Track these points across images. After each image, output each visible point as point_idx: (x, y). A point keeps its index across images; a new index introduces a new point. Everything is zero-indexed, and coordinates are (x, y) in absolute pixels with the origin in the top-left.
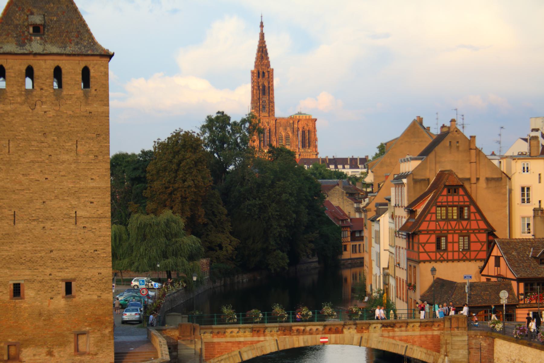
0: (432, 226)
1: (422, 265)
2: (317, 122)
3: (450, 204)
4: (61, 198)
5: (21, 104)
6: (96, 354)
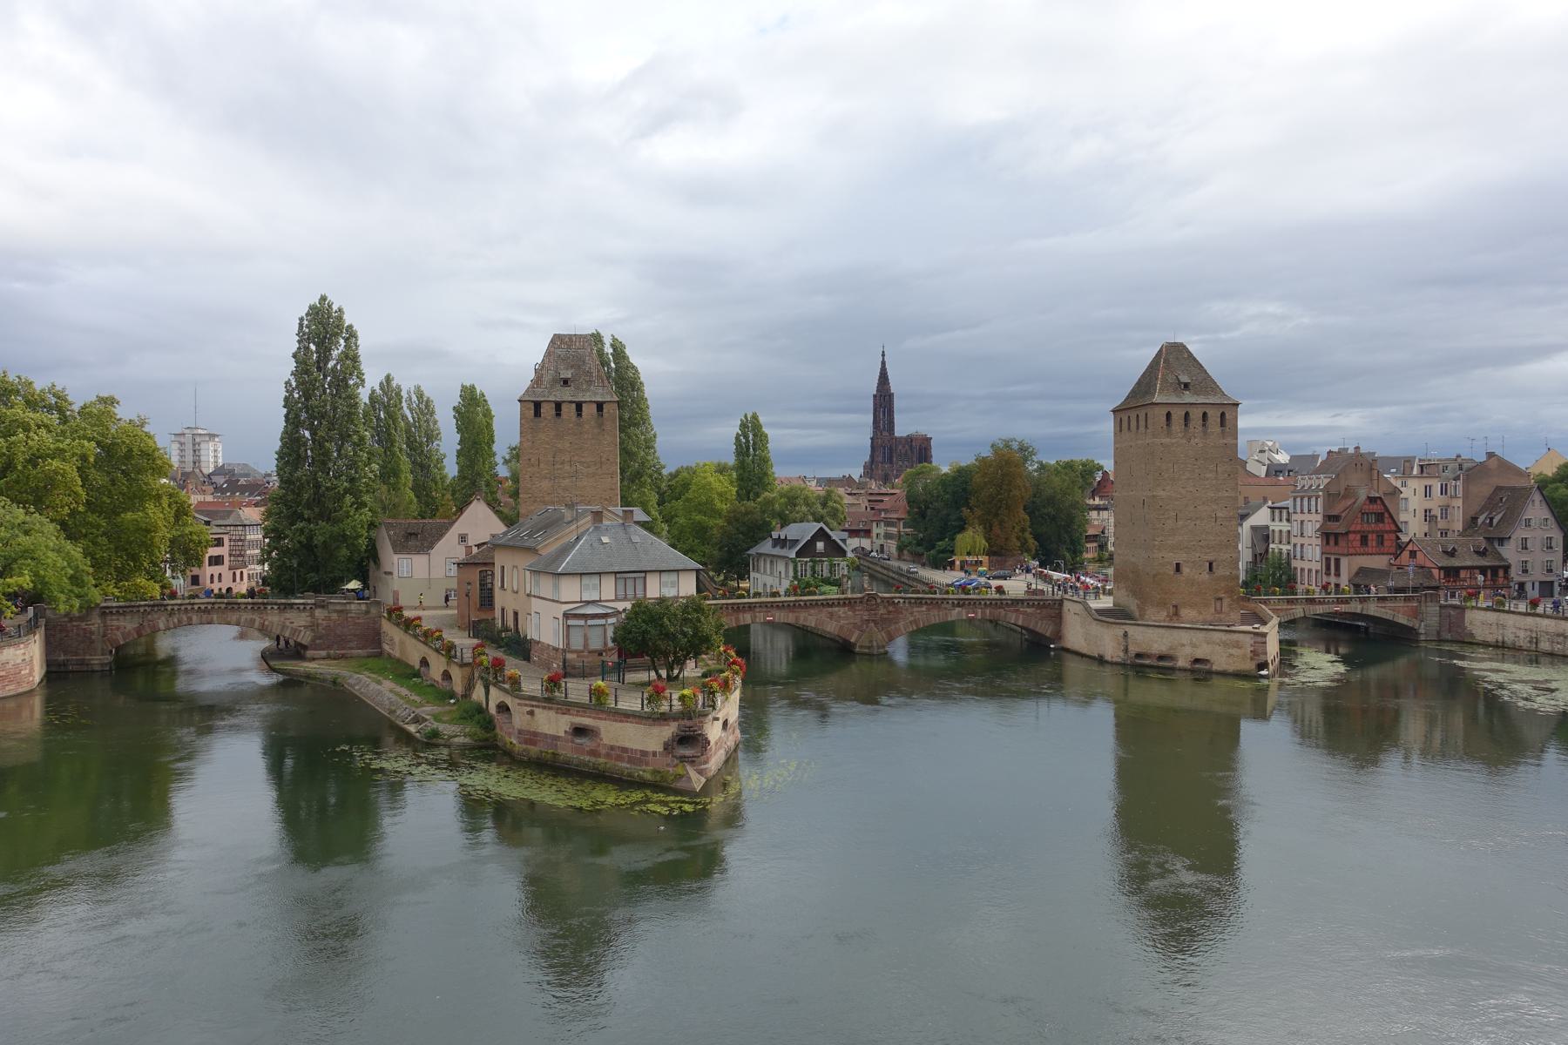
0: (1358, 528)
2: (932, 441)
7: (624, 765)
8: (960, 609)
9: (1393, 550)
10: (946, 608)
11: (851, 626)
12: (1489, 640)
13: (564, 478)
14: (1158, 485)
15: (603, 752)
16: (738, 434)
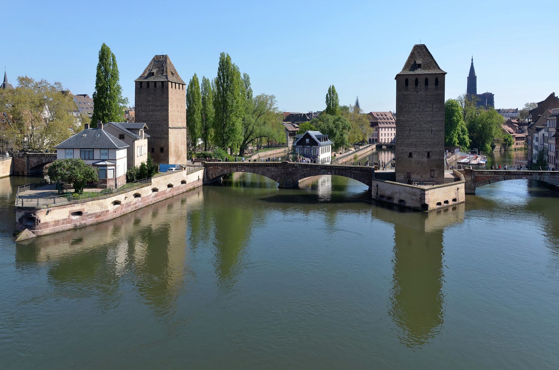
6: (438, 178)
8: (325, 170)
10: (318, 170)
11: (276, 175)
13: (150, 111)
16: (327, 94)
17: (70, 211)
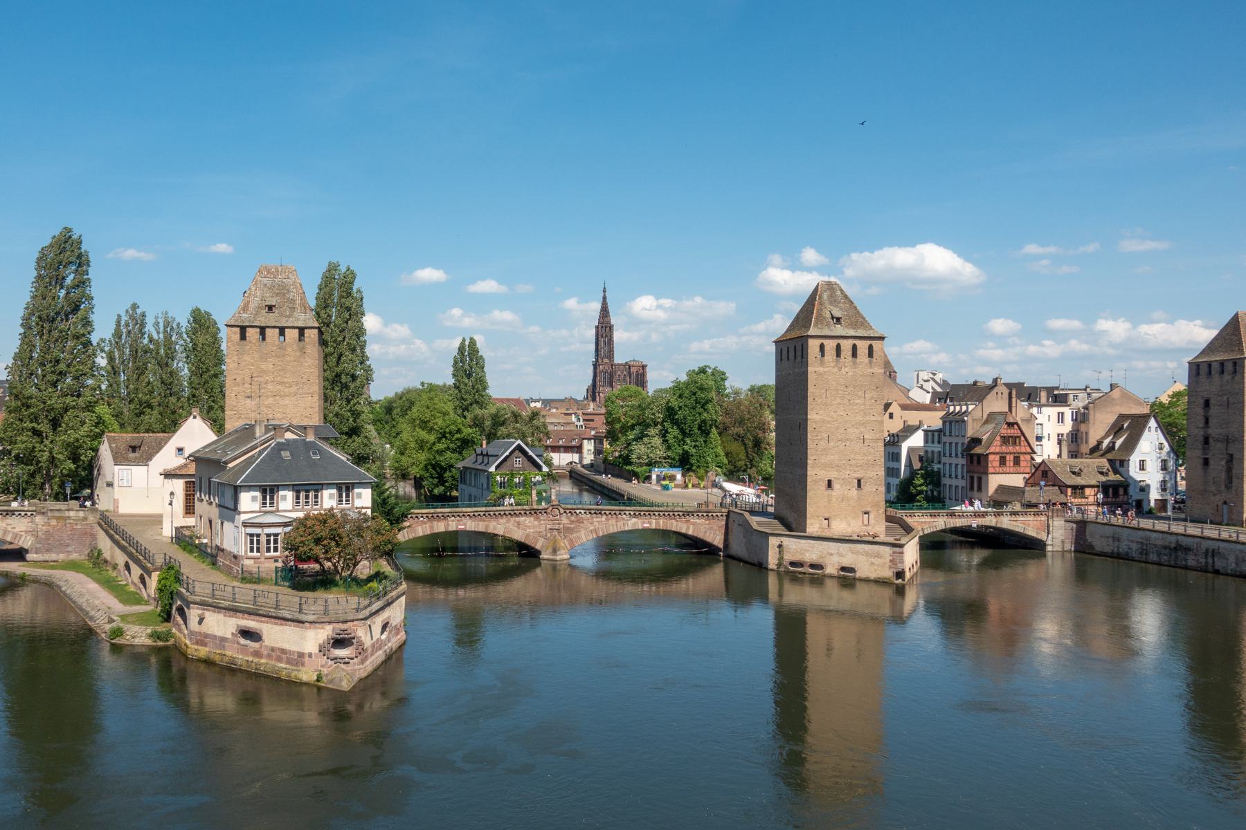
0: (998, 450)
1: (990, 475)
3: (1009, 435)
4: (855, 426)
5: (833, 367)
7: (283, 665)
9: (1028, 470)
10: (623, 519)
12: (1105, 551)
14: (813, 409)
15: (265, 653)
17: (382, 622)
